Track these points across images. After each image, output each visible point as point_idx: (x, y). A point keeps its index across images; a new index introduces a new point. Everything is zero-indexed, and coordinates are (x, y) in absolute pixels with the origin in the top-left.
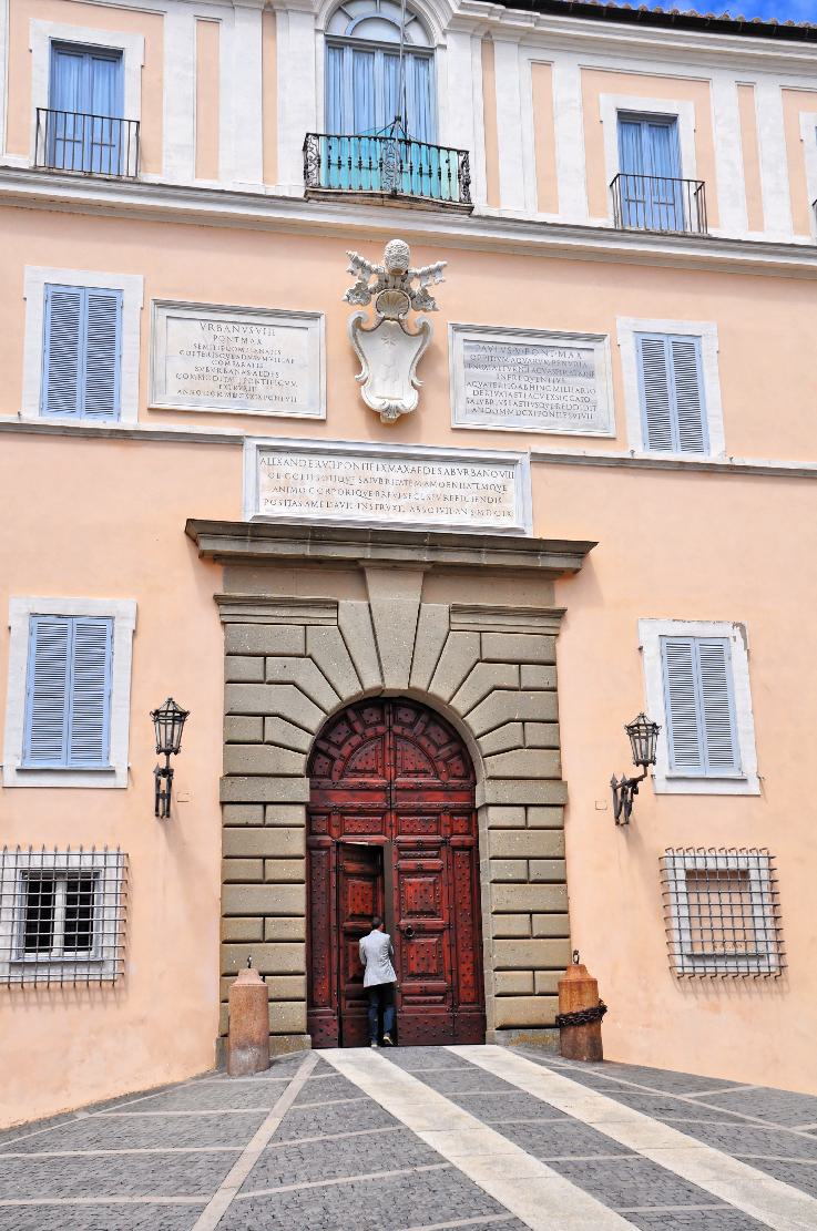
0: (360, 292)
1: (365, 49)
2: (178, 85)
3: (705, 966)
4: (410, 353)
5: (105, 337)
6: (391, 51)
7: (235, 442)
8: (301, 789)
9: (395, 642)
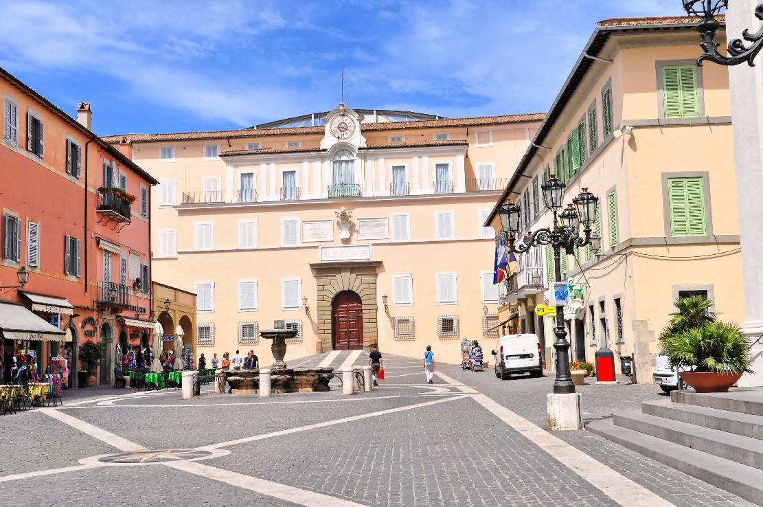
5: (294, 230)
6: (347, 162)
7: (317, 247)
8: (330, 309)
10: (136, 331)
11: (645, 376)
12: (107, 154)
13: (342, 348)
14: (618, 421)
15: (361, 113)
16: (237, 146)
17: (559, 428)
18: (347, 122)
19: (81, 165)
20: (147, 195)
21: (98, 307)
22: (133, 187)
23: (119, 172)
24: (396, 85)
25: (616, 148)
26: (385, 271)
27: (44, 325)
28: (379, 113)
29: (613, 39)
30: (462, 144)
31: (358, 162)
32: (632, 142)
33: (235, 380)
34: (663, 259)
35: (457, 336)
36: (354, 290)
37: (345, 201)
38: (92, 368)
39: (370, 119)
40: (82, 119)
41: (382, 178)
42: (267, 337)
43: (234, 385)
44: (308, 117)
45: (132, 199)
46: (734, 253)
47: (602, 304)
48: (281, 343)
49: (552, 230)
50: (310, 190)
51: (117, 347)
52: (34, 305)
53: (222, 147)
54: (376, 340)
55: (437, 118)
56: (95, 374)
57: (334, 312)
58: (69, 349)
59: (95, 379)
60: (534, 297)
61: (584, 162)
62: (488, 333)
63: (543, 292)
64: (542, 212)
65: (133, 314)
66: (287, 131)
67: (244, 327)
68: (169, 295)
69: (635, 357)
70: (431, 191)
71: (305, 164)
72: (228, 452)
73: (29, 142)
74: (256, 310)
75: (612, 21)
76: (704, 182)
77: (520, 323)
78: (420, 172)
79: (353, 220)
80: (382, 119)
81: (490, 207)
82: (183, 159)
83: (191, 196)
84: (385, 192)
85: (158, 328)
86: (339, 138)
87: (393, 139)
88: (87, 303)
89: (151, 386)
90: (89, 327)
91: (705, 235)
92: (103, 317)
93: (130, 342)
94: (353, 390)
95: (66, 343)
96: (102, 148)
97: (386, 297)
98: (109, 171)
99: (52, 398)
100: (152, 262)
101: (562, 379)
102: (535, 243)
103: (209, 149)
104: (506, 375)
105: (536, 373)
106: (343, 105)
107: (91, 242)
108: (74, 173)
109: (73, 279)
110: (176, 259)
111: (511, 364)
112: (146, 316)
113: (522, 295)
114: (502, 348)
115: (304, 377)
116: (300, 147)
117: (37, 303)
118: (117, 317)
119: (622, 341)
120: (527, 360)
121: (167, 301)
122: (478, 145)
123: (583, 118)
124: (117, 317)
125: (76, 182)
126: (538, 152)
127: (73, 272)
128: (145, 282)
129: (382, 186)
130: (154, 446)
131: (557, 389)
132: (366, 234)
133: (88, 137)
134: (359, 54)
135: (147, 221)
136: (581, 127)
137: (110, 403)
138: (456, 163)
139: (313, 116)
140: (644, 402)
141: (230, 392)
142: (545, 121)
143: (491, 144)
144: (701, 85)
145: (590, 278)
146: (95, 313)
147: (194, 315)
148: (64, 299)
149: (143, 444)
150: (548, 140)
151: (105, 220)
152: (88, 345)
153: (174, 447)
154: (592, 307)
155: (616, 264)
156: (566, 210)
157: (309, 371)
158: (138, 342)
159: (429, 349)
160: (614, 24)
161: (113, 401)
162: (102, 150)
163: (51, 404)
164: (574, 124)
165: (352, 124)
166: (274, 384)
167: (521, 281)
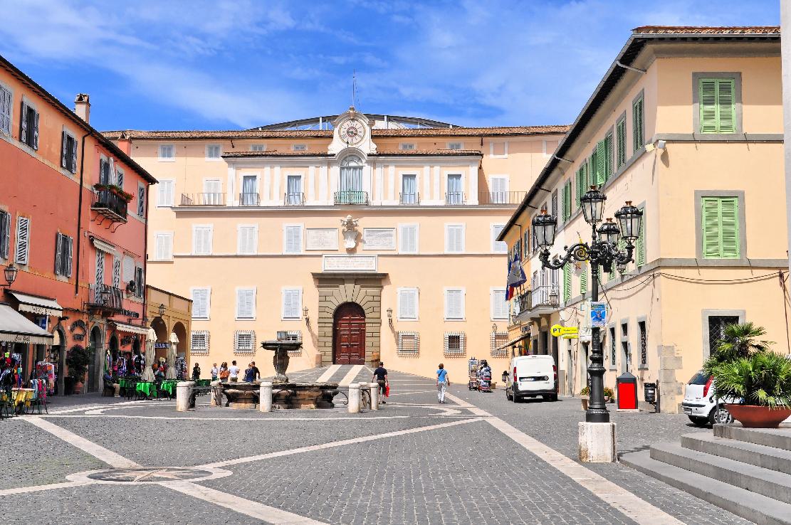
0: (343, 225)
1: (349, 168)
2: (311, 181)
3: (403, 351)
4: (354, 234)
6: (355, 168)
7: (321, 256)
8: (332, 321)
9: (350, 292)
10: (127, 337)
11: (670, 405)
12: (104, 148)
13: (343, 363)
14: (655, 455)
15: (372, 118)
16: (241, 147)
17: (591, 459)
18: (357, 127)
19: (77, 161)
20: (144, 194)
21: (88, 310)
22: (130, 185)
23: (116, 169)
24: (406, 92)
25: (647, 162)
26: (390, 283)
27: (35, 328)
28: (390, 119)
29: (649, 48)
30: (477, 154)
31: (367, 169)
32: (665, 157)
33: (233, 393)
34: (691, 281)
35: (463, 355)
36: (358, 302)
37: (351, 209)
38: (80, 374)
39: (380, 125)
40: (80, 111)
41: (391, 187)
42: (268, 349)
43: (233, 398)
44: (316, 120)
45: (129, 197)
46: (771, 278)
47: (625, 327)
48: (283, 355)
49: (590, 245)
50: (316, 198)
51: (107, 353)
52: (21, 305)
53: (225, 147)
54: (379, 356)
55: (451, 127)
56: (82, 381)
57: (335, 325)
58: (56, 352)
59: (82, 386)
60: (548, 317)
61: (610, 178)
62: (500, 353)
63: (559, 311)
64: (560, 228)
65: (124, 319)
66: (294, 134)
67: (241, 337)
68: (164, 300)
69: (660, 385)
70: (442, 203)
71: (312, 169)
72: (229, 473)
73: (23, 132)
74: (254, 319)
75: (648, 28)
76: (739, 201)
77: (531, 343)
78: (431, 182)
79: (360, 229)
80: (393, 126)
81: (504, 221)
82: (183, 159)
83: (190, 197)
84: (393, 201)
85: (151, 335)
86: (348, 143)
87: (405, 147)
88: (77, 305)
89: (142, 396)
90: (78, 331)
91: (738, 257)
92: (94, 320)
93: (120, 348)
94: (359, 408)
95: (53, 346)
96: (100, 142)
97: (391, 311)
98: (105, 167)
99: (37, 405)
100: (148, 265)
101: (596, 407)
102: (572, 258)
103: (211, 148)
104: (519, 397)
105: (550, 396)
106: (353, 109)
107: (84, 243)
108: (69, 167)
109: (63, 279)
110: (172, 262)
111: (524, 386)
112: (139, 322)
113: (536, 314)
114: (515, 368)
115: (307, 392)
116: (307, 151)
117: (24, 303)
118: (108, 321)
119: (646, 366)
120: (542, 382)
121: (162, 306)
122: (492, 156)
123: (611, 131)
124: (108, 321)
125: (72, 177)
126: (560, 165)
127: (64, 270)
128: (139, 286)
129: (391, 195)
130: (149, 463)
131: (590, 418)
132: (372, 243)
133: (85, 130)
134: (369, 59)
135: (144, 221)
136: (607, 141)
137: (99, 412)
138: (470, 173)
139: (321, 119)
140: (683, 436)
141: (227, 405)
142: (568, 135)
143: (506, 155)
144: (739, 100)
145: (612, 298)
146: (85, 316)
147: (188, 322)
148: (53, 300)
149: (136, 460)
150: (571, 152)
151: (100, 218)
152: (77, 349)
153: (168, 464)
154: (613, 330)
155: (643, 285)
156: (606, 224)
157: (313, 386)
158: (129, 348)
159: (441, 367)
160: (651, 32)
161: (102, 410)
162: (100, 145)
163: (36, 411)
164: (600, 137)
165: (362, 130)
166: (275, 399)
167: (536, 300)
